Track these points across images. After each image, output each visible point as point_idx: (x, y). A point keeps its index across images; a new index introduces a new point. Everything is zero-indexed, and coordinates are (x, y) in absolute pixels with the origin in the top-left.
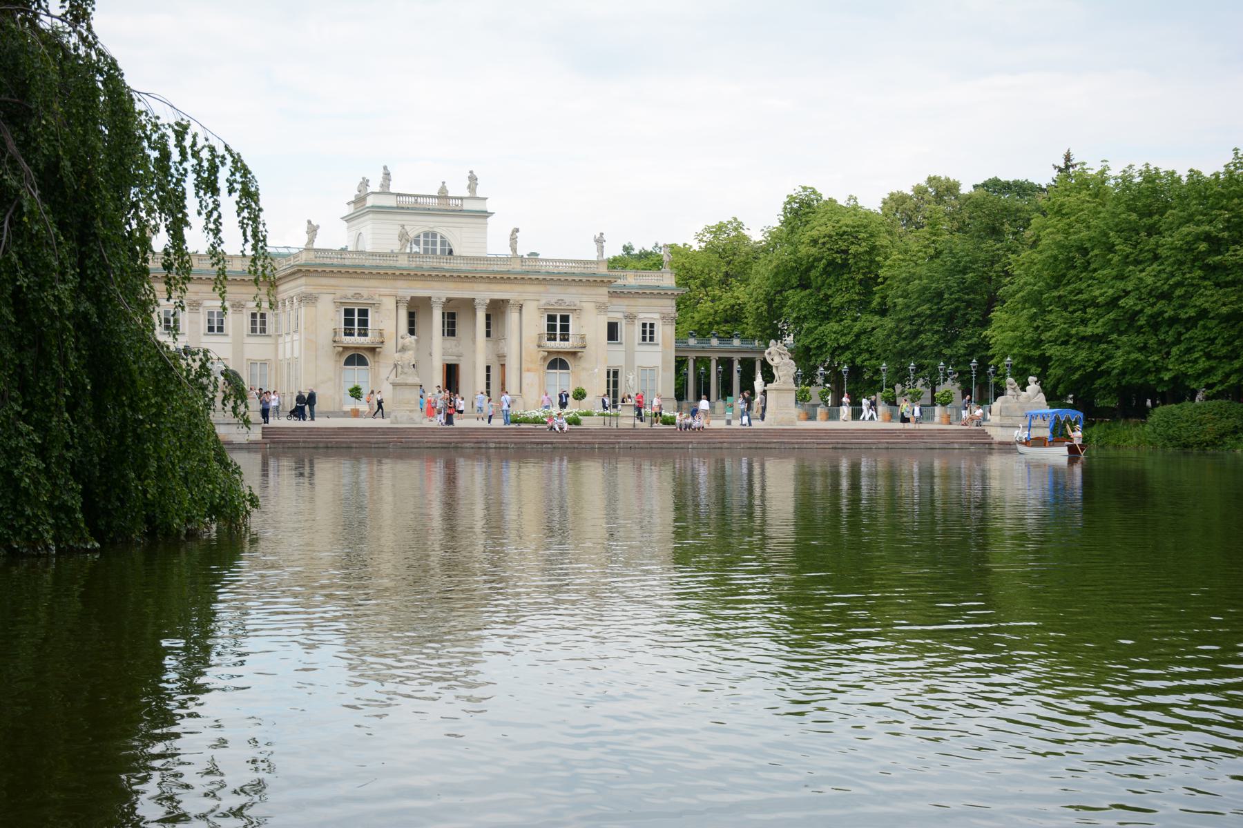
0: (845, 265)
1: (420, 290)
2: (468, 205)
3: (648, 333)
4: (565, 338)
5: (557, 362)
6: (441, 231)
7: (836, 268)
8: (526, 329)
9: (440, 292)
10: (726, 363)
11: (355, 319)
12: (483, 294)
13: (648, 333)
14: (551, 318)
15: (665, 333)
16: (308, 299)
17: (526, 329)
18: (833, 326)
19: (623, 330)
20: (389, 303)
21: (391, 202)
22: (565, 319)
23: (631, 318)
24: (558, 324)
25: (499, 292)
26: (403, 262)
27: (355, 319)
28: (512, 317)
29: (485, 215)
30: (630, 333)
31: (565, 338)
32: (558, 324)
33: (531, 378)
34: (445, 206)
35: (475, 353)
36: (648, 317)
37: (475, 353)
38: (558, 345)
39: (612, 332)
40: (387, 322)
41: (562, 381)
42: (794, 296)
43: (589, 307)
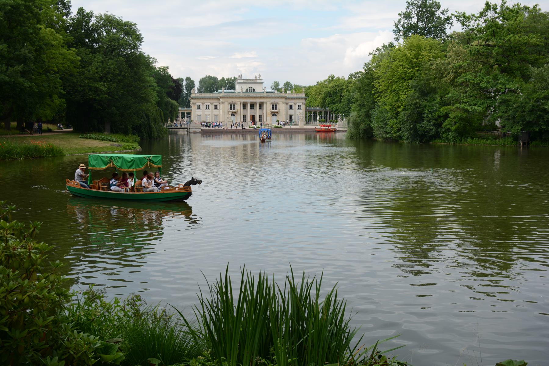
0: (336, 92)
1: (245, 100)
2: (258, 81)
3: (299, 107)
4: (276, 109)
5: (274, 114)
6: (253, 87)
7: (335, 93)
8: (268, 107)
9: (249, 101)
10: (315, 113)
11: (232, 107)
12: (258, 101)
13: (299, 107)
14: (273, 105)
15: (303, 107)
16: (223, 103)
17: (268, 107)
18: (335, 105)
19: (293, 107)
20: (239, 103)
21: (242, 81)
22: (276, 105)
23: (295, 104)
24: (274, 107)
25: (262, 100)
26: (241, 95)
27: (232, 107)
28: (265, 105)
29: (262, 83)
30: (295, 107)
31: (276, 109)
32: (274, 107)
33: (269, 118)
34: (255, 81)
35: (257, 112)
36: (299, 104)
37: (257, 112)
38: (274, 111)
39: (291, 107)
40: (239, 107)
41: (275, 118)
42: (328, 99)
43: (281, 103)
